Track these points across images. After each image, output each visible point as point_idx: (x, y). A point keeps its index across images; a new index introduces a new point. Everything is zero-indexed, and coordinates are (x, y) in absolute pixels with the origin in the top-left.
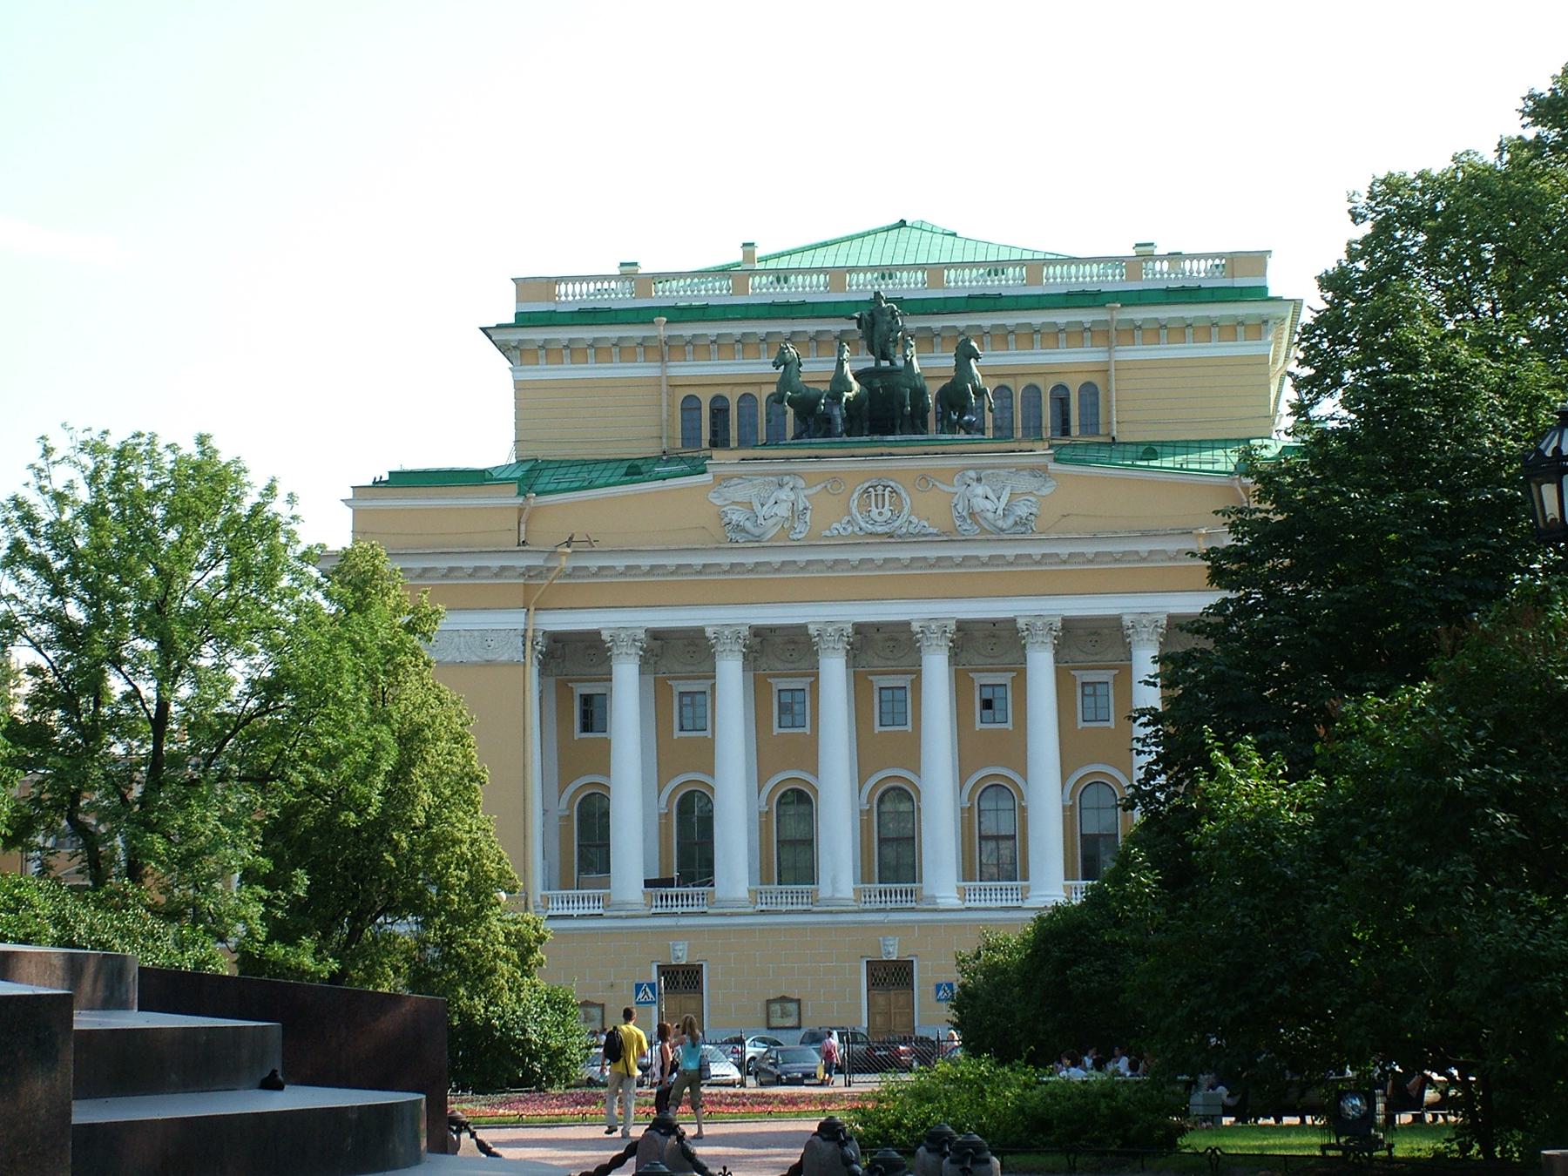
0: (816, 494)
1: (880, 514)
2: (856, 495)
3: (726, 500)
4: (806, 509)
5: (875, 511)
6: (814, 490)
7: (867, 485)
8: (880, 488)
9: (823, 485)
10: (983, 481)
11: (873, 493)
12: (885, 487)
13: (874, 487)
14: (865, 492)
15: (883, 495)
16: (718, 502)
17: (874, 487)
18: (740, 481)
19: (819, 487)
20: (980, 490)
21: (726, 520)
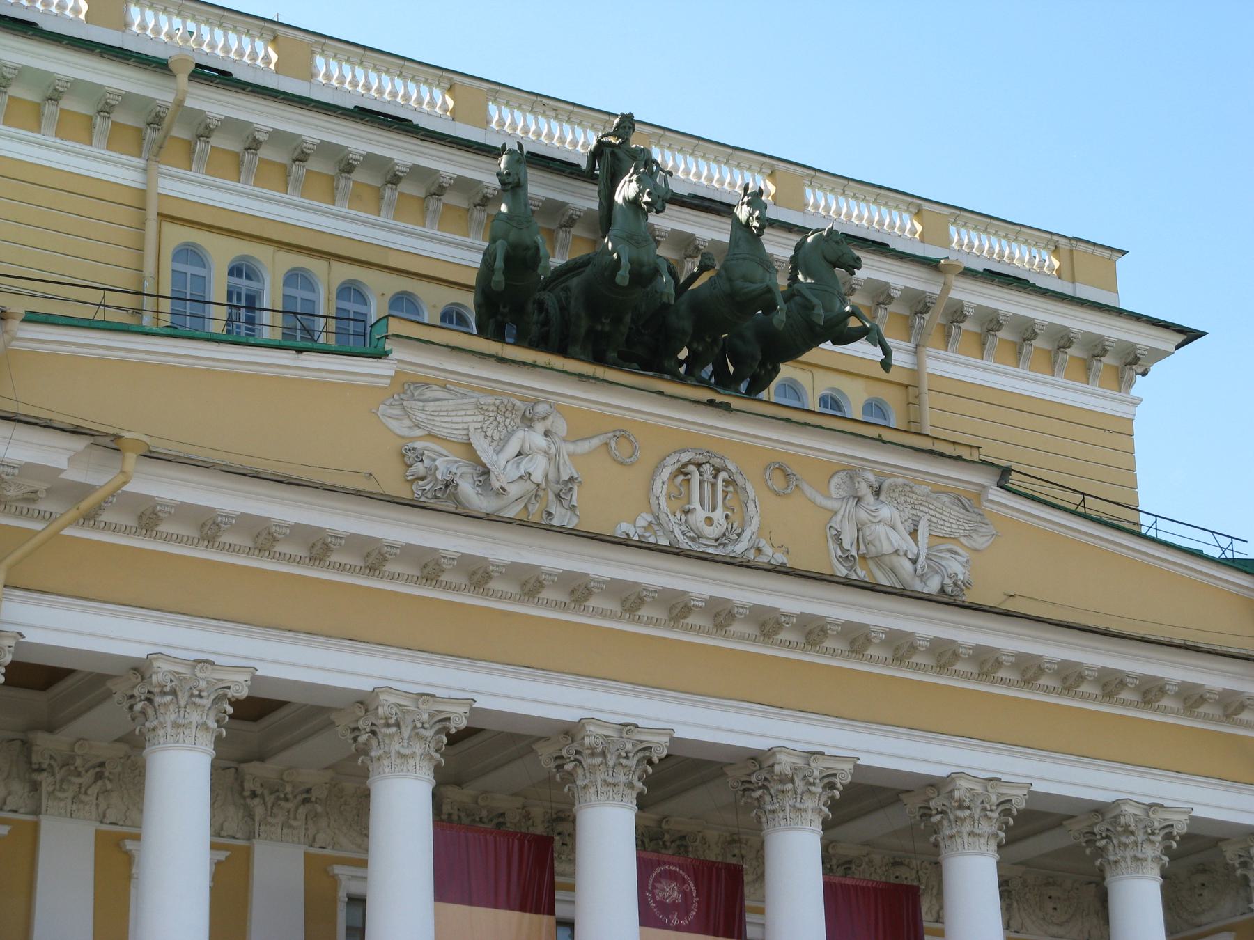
0: (589, 453)
1: (709, 521)
2: (666, 473)
3: (418, 426)
4: (572, 479)
5: (699, 516)
6: (584, 447)
7: (685, 457)
8: (707, 469)
9: (596, 442)
10: (882, 497)
11: (696, 479)
12: (717, 471)
13: (699, 465)
14: (682, 471)
15: (713, 485)
16: (400, 427)
17: (699, 465)
18: (440, 394)
19: (596, 442)
20: (886, 512)
21: (420, 468)
